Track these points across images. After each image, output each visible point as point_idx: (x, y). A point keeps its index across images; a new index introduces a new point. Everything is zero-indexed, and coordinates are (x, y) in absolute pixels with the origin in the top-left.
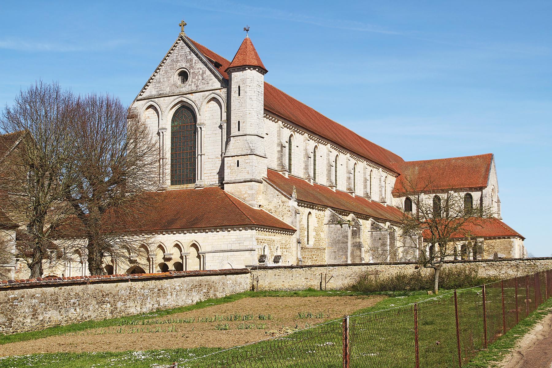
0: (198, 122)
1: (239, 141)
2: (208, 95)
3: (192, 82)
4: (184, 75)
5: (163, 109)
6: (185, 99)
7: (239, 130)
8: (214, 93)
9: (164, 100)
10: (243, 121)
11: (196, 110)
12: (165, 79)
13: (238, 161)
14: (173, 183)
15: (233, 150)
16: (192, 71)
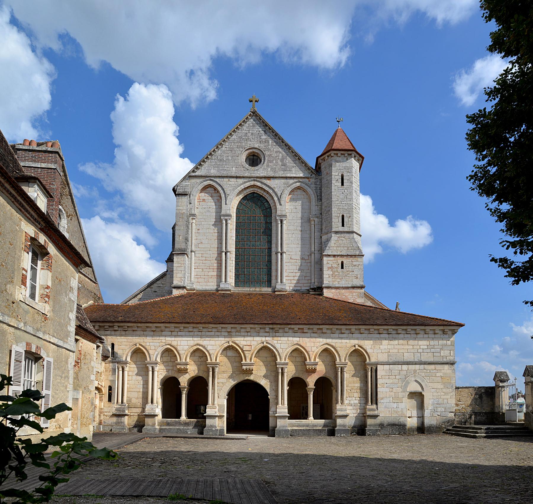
0: (279, 213)
1: (343, 239)
2: (293, 183)
3: (268, 166)
4: (254, 159)
5: (228, 192)
6: (259, 184)
7: (343, 225)
8: (299, 182)
9: (229, 181)
10: (348, 215)
11: (276, 199)
12: (230, 158)
13: (342, 263)
14: (237, 284)
15: (335, 248)
16: (267, 153)
